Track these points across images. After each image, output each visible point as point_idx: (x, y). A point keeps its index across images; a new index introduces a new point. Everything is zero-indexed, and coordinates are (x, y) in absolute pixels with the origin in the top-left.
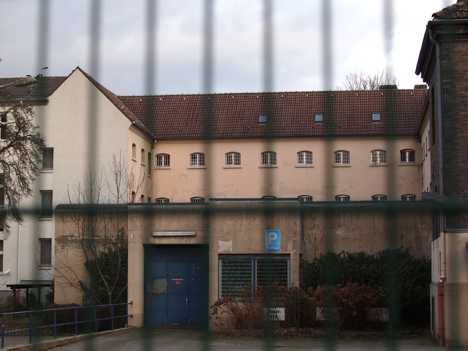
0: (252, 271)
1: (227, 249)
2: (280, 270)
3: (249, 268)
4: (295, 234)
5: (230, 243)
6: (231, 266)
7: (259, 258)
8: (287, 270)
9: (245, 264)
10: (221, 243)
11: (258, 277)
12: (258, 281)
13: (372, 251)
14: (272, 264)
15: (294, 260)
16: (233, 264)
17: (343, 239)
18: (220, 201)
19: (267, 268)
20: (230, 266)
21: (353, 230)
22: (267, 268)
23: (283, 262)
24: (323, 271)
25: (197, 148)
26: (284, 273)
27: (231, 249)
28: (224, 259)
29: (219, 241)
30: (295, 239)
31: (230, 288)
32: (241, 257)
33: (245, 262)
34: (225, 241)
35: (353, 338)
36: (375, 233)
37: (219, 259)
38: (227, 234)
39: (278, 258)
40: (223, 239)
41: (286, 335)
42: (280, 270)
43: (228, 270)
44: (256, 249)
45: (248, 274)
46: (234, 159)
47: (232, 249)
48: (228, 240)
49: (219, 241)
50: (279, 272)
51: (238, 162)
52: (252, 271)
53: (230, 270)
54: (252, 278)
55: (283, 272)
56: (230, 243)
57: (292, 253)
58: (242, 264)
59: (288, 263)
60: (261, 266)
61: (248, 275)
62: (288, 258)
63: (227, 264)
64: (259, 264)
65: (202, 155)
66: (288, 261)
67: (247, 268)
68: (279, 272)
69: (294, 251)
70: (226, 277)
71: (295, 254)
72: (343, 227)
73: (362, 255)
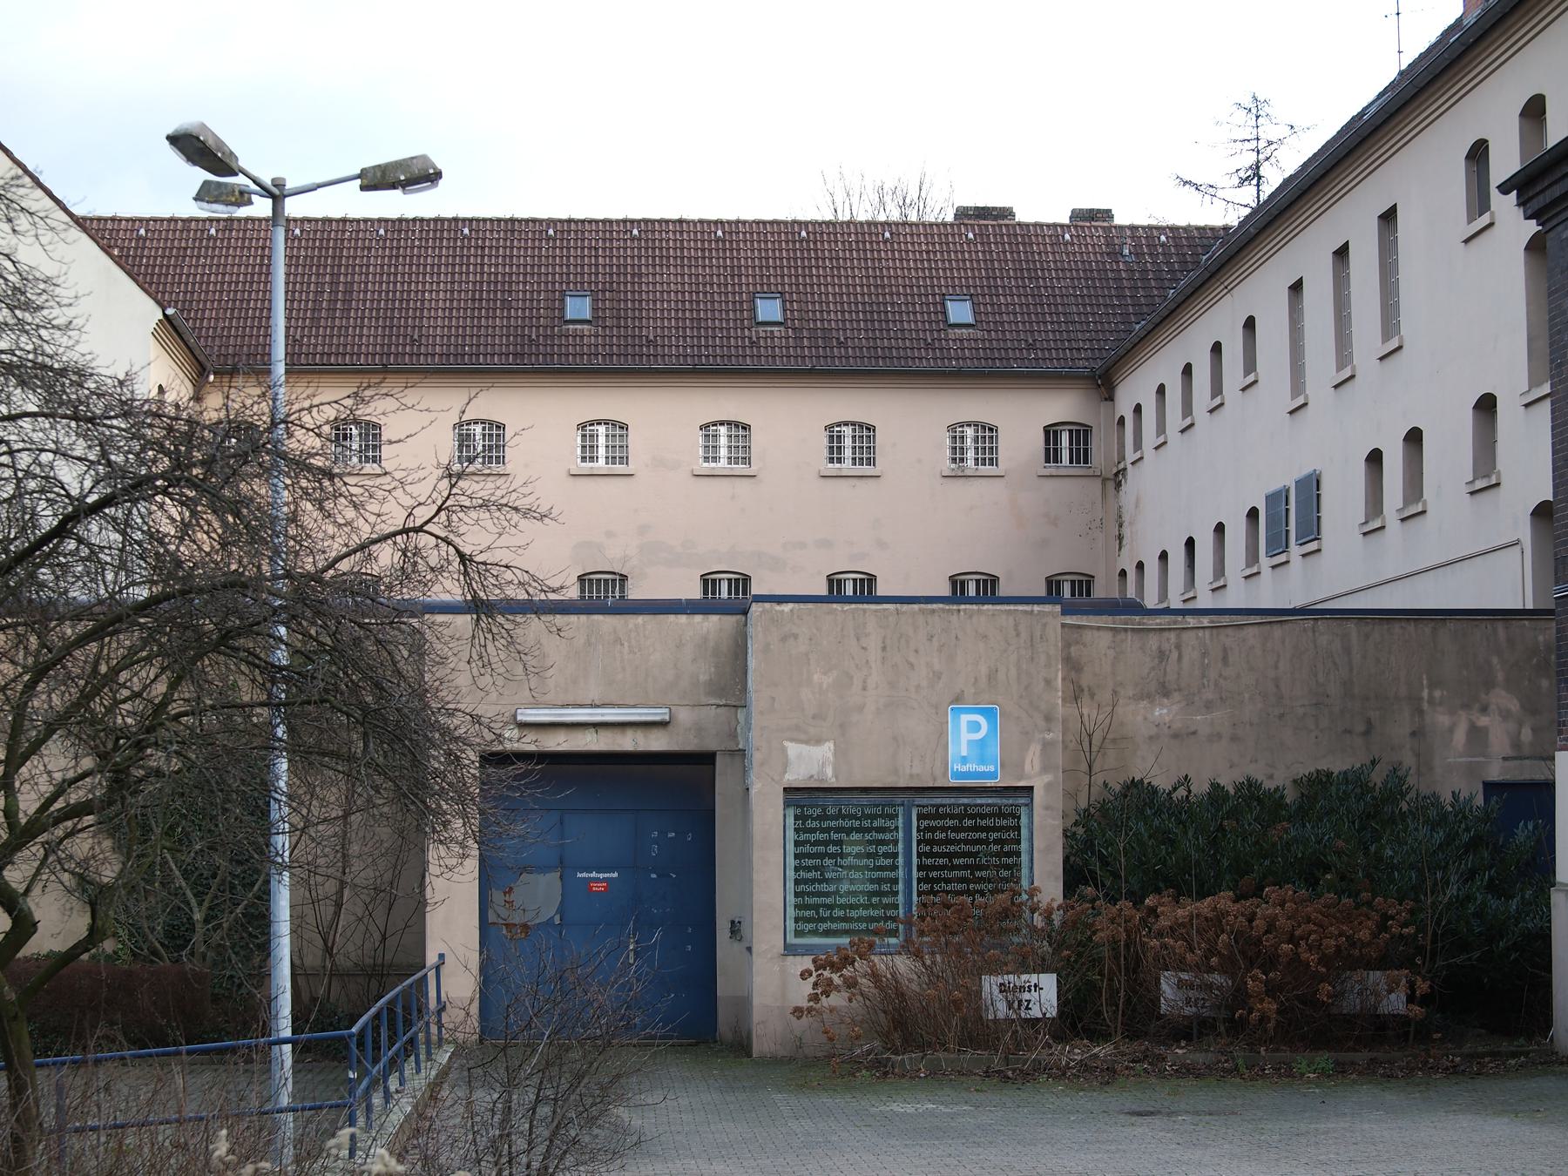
0: (900, 846)
1: (814, 772)
2: (996, 842)
3: (888, 836)
4: (1048, 718)
5: (827, 749)
6: (827, 830)
7: (925, 801)
8: (1018, 842)
9: (875, 824)
10: (793, 749)
11: (920, 868)
12: (919, 880)
13: (1271, 777)
14: (968, 823)
15: (1047, 808)
16: (833, 824)
17: (1176, 736)
18: (791, 606)
19: (952, 835)
20: (823, 831)
21: (1209, 706)
22: (952, 835)
23: (1005, 816)
24: (1132, 841)
25: (1061, 406)
26: (1009, 854)
27: (829, 772)
28: (802, 807)
29: (786, 744)
30: (1049, 736)
31: (825, 906)
32: (864, 799)
33: (873, 817)
34: (807, 742)
35: (1323, 1074)
36: (1281, 716)
37: (787, 804)
38: (814, 717)
39: (990, 801)
40: (803, 737)
41: (1086, 1068)
42: (996, 842)
43: (817, 843)
44: (915, 771)
45: (886, 855)
46: (855, 447)
47: (835, 770)
48: (818, 741)
49: (786, 744)
50: (995, 848)
51: (866, 455)
52: (900, 846)
53: (826, 843)
54: (901, 873)
55: (1006, 848)
56: (827, 749)
57: (1039, 784)
58: (866, 823)
59: (1024, 820)
60: (932, 830)
61: (888, 862)
62: (1022, 801)
63: (815, 824)
64: (926, 823)
65: (1081, 434)
66: (1023, 812)
67: (881, 836)
68: (995, 848)
69: (1048, 778)
70: (809, 869)
71: (1048, 787)
72: (1176, 696)
73: (1250, 790)
